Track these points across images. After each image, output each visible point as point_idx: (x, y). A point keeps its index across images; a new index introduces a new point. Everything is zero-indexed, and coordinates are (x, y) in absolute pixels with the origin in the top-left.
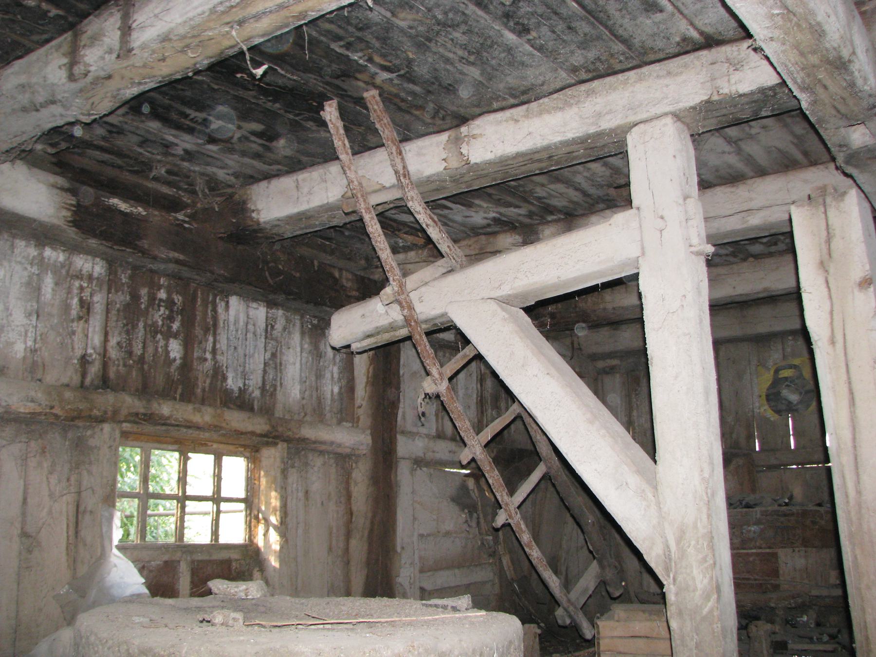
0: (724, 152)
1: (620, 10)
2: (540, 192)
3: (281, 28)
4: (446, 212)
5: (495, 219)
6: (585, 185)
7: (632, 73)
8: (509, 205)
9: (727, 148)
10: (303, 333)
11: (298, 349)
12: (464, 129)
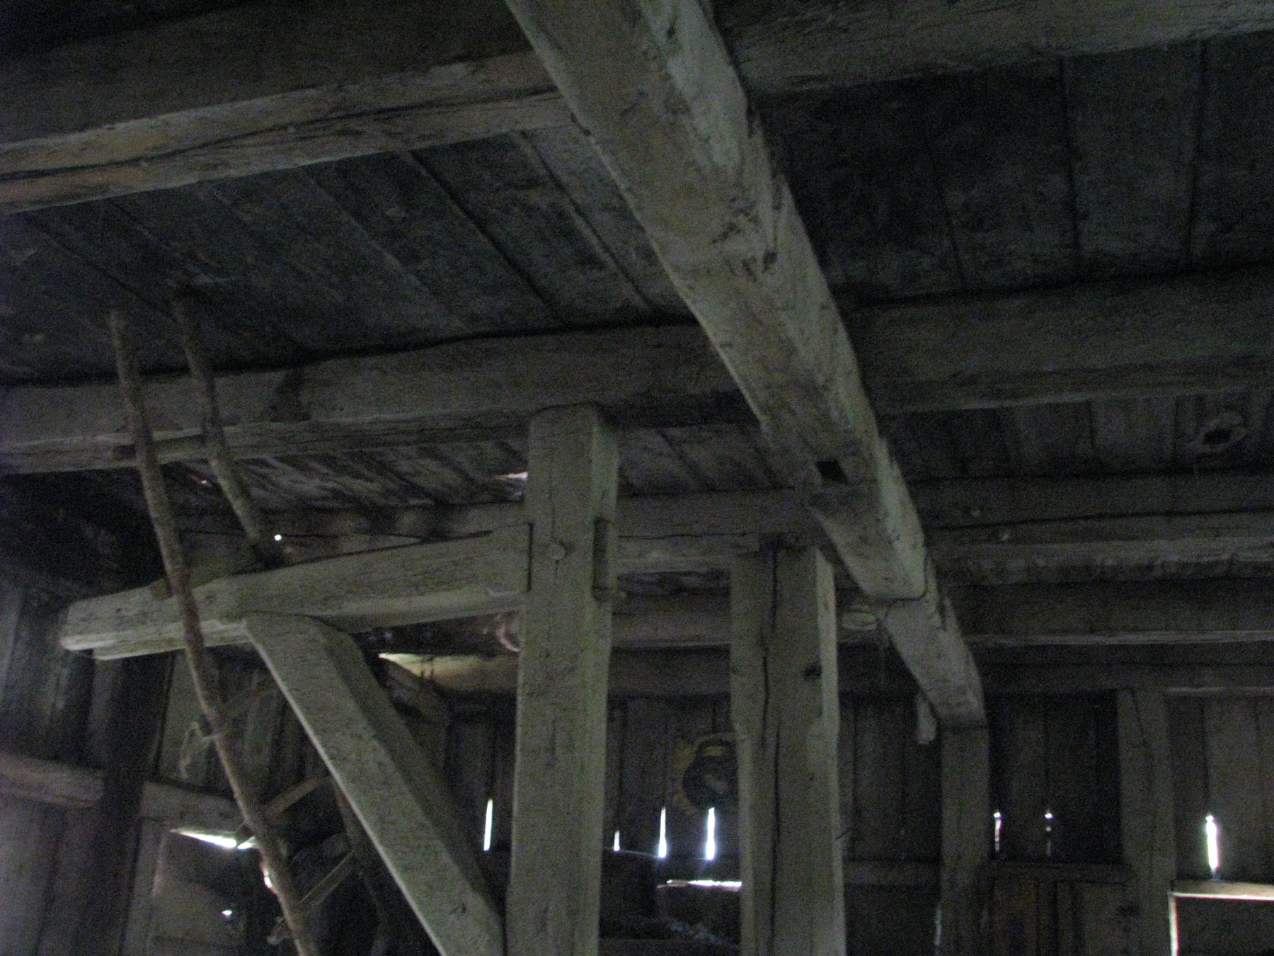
0: (661, 454)
1: (547, 256)
2: (404, 466)
3: (66, 197)
4: (265, 471)
5: (333, 490)
6: (467, 467)
7: (550, 339)
8: (358, 476)
9: (666, 449)
10: (23, 612)
11: (11, 638)
12: (309, 371)
